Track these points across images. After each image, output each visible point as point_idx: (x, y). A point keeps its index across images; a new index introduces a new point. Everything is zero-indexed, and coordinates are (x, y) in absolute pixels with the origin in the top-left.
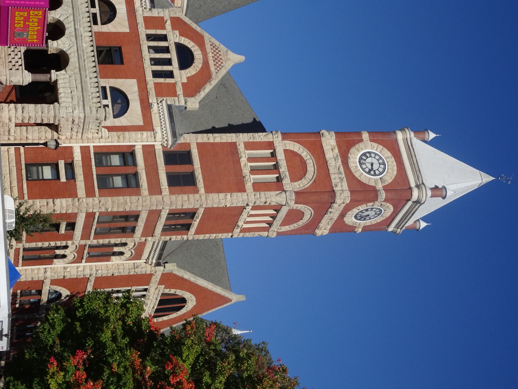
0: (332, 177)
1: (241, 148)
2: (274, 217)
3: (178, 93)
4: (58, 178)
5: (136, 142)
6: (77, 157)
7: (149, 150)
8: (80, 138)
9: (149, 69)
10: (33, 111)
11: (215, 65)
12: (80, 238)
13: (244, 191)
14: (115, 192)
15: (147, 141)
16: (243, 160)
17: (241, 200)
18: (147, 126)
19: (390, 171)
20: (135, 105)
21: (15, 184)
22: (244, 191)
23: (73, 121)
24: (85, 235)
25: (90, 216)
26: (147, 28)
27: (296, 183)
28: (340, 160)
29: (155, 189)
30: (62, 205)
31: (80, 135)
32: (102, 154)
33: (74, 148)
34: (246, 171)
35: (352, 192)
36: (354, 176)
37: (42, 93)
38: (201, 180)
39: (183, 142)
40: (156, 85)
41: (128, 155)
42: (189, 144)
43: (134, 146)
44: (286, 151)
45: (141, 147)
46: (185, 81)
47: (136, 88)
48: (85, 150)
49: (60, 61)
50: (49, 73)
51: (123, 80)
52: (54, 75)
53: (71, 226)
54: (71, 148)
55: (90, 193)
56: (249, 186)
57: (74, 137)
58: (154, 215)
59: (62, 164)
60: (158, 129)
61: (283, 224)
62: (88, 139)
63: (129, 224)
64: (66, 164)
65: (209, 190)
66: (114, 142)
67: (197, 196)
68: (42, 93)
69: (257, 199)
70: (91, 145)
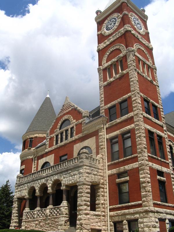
0: (118, 37)
1: (106, 83)
2: (144, 63)
3: (80, 122)
4: (126, 182)
5: (104, 138)
6: (114, 171)
7: (109, 130)
8: (102, 171)
9: (70, 139)
10: (83, 199)
11: (69, 109)
12: (168, 169)
13: (128, 73)
14: (134, 143)
15: (104, 132)
16: (112, 80)
17: (133, 73)
18: (95, 134)
19: (114, 16)
20: (86, 143)
21: (132, 211)
22: (128, 73)
23: (88, 173)
24: (167, 165)
25: (151, 159)
26: (53, 145)
27: (122, 51)
28: (110, 37)
29: (131, 120)
30: (145, 177)
31: (100, 171)
32: (112, 156)
33: (109, 174)
34: (118, 76)
35: (124, 25)
36: (117, 28)
37: (72, 193)
38: (124, 97)
39: (104, 113)
40: (76, 134)
41: (111, 142)
42: (105, 110)
43: (107, 139)
44: (106, 63)
45: (107, 135)
46: (75, 120)
47: (78, 145)
48: (110, 167)
49: (57, 184)
50: (62, 191)
51: (74, 152)
52: (63, 188)
53: (161, 173)
54: (109, 176)
55: (135, 159)
56: (125, 72)
57: (101, 174)
58: (146, 120)
59: (118, 180)
60: (97, 128)
61: (148, 61)
62: (103, 166)
63: (156, 139)
64: (119, 178)
65: (129, 91)
66: (105, 151)
67: (132, 96)
68: (72, 193)
69: (132, 65)
70: (107, 164)
